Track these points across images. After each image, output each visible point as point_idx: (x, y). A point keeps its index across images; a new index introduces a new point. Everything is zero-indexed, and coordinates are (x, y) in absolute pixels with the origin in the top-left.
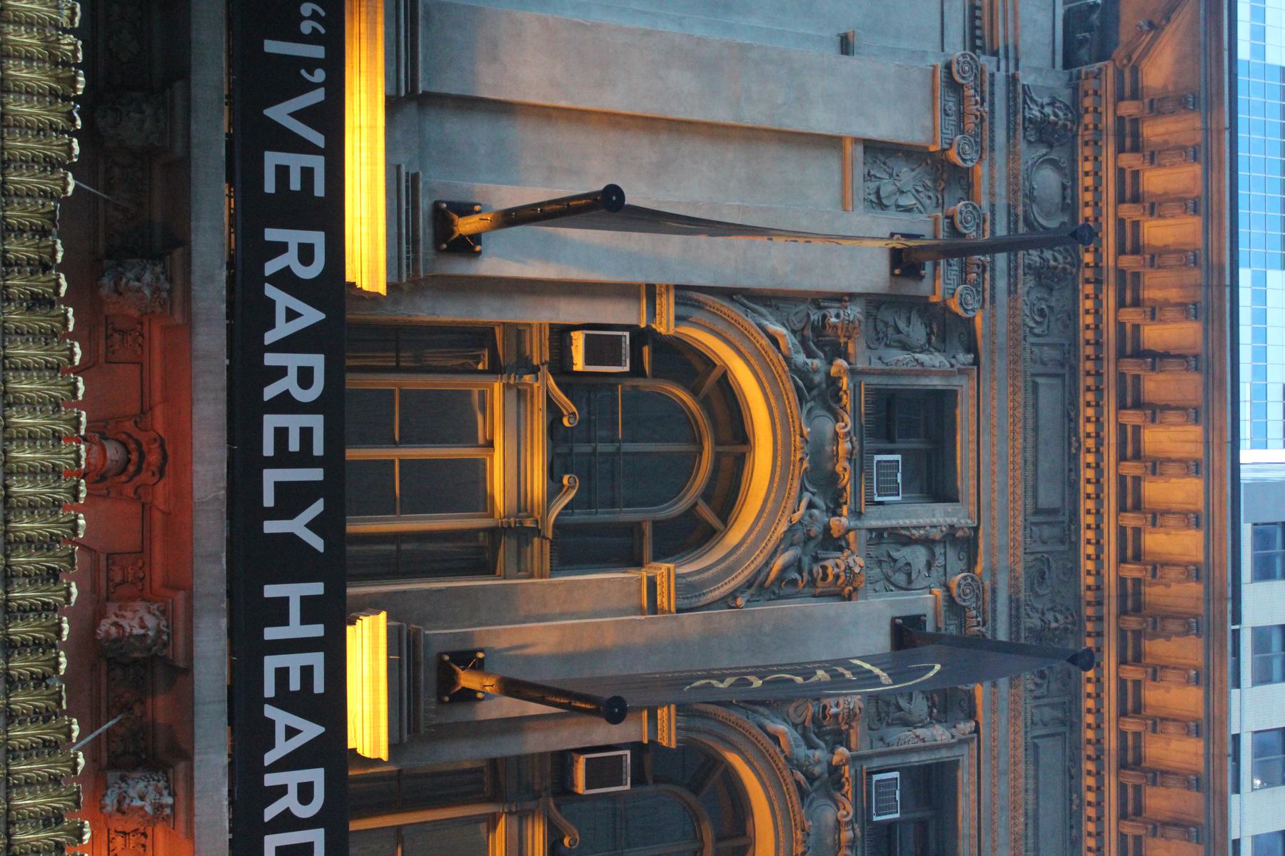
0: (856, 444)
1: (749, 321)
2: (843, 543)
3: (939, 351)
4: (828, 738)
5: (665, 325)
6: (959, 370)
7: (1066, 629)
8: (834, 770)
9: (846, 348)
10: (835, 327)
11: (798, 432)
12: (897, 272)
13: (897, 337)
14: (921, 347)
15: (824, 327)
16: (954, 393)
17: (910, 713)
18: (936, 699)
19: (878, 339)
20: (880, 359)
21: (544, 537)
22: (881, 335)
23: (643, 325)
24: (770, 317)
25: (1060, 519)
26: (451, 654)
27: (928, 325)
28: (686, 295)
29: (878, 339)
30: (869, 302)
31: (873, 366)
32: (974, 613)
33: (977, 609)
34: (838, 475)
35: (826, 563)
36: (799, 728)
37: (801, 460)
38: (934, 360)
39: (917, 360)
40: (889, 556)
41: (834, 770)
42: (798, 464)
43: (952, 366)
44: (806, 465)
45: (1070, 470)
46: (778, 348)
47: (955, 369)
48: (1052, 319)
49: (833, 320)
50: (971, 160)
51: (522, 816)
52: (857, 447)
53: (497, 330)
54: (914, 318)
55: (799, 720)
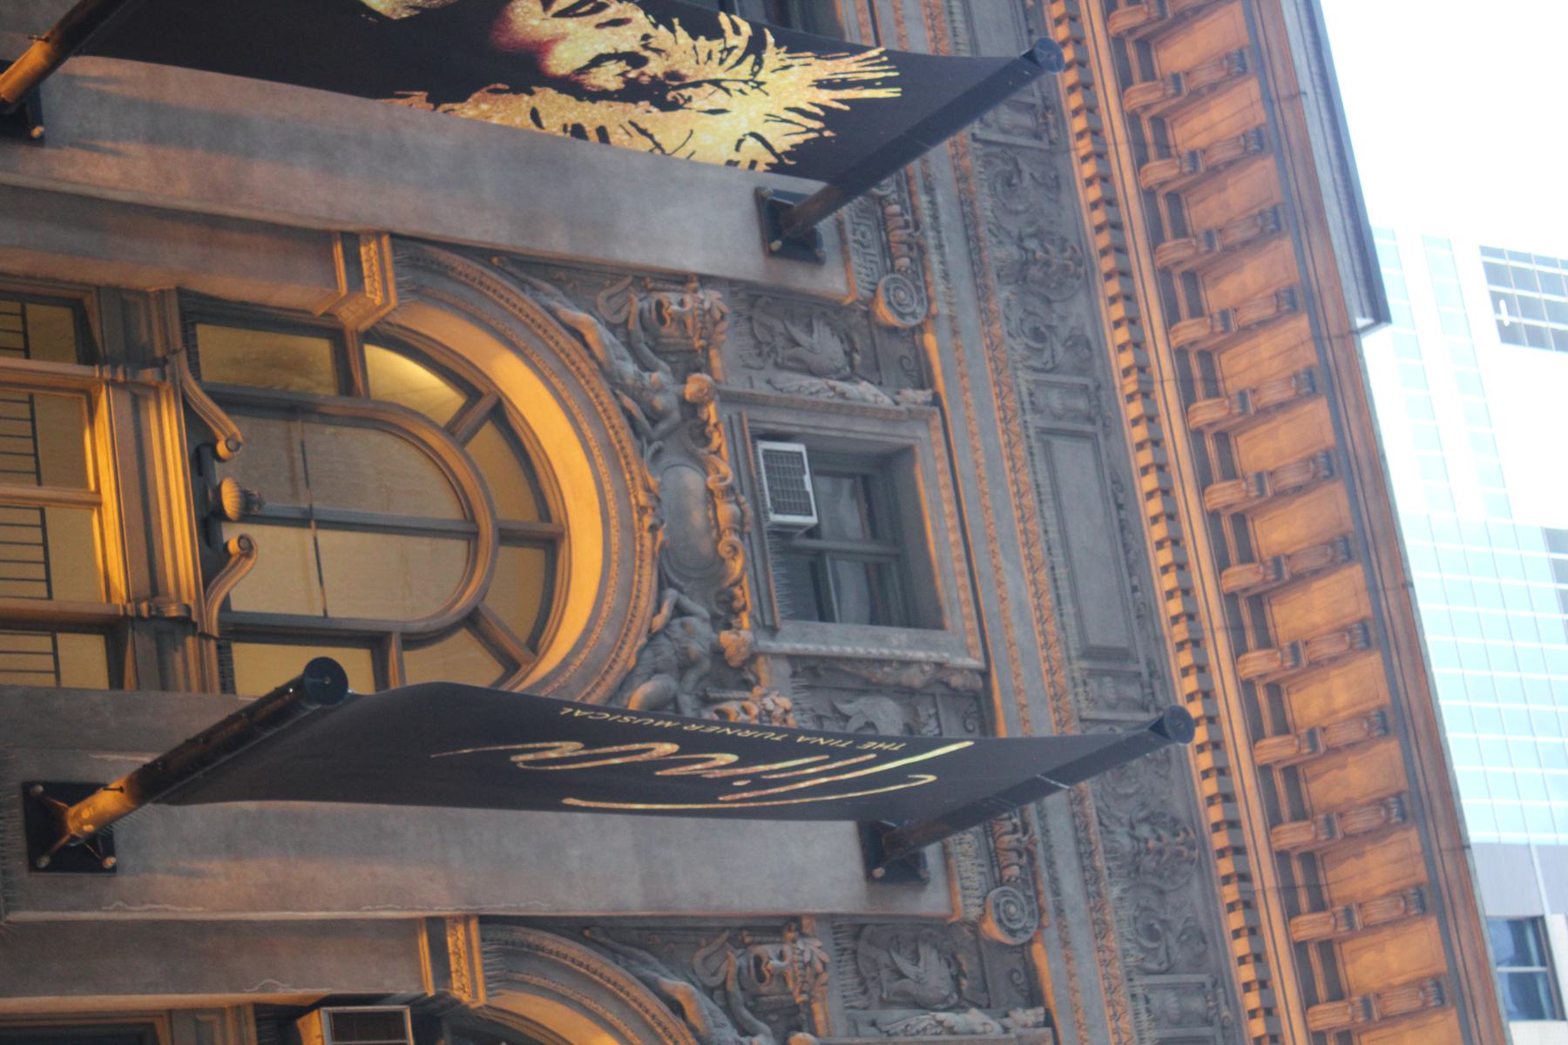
0: (748, 506)
1: (527, 302)
2: (751, 677)
3: (979, 1007)
4: (673, 359)
5: (469, 987)
6: (1019, 1037)
7: (1179, 854)
8: (691, 408)
9: (708, 358)
10: (680, 321)
11: (638, 481)
12: (879, 872)
13: (791, 352)
14: (945, 1000)
15: (662, 320)
16: (906, 452)
17: (919, 981)
18: (857, 338)
19: (760, 354)
20: (769, 382)
21: (206, 636)
22: (766, 349)
23: (431, 993)
24: (665, 970)
25: (1132, 667)
26: (45, 784)
27: (846, 338)
28: (511, 937)
29: (760, 354)
30: (837, 930)
31: (756, 391)
32: (896, 208)
33: (902, 203)
34: (723, 560)
35: (724, 706)
36: (718, 993)
37: (653, 529)
38: (864, 391)
39: (940, 1023)
40: (835, 710)
41: (691, 408)
42: (647, 536)
43: (897, 403)
44: (661, 536)
45: (1134, 589)
46: (586, 345)
47: (1012, 1035)
48: (1172, 941)
49: (775, 962)
50: (914, 315)
51: (138, 398)
52: (750, 513)
53: (87, 302)
54: (924, 950)
55: (620, 318)
